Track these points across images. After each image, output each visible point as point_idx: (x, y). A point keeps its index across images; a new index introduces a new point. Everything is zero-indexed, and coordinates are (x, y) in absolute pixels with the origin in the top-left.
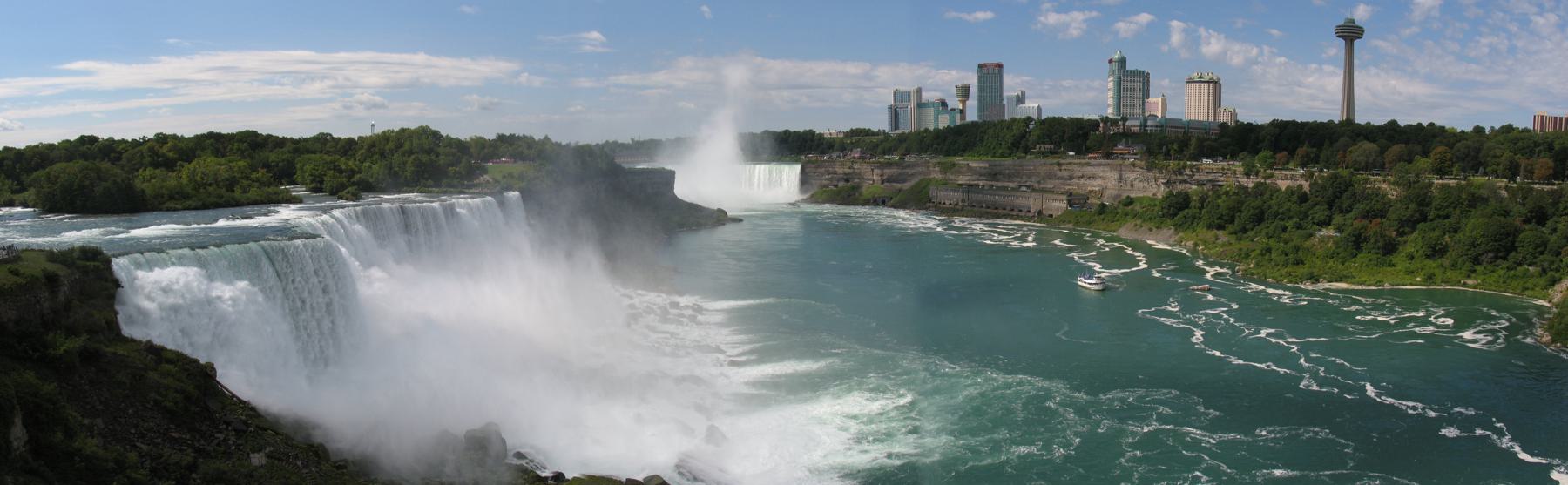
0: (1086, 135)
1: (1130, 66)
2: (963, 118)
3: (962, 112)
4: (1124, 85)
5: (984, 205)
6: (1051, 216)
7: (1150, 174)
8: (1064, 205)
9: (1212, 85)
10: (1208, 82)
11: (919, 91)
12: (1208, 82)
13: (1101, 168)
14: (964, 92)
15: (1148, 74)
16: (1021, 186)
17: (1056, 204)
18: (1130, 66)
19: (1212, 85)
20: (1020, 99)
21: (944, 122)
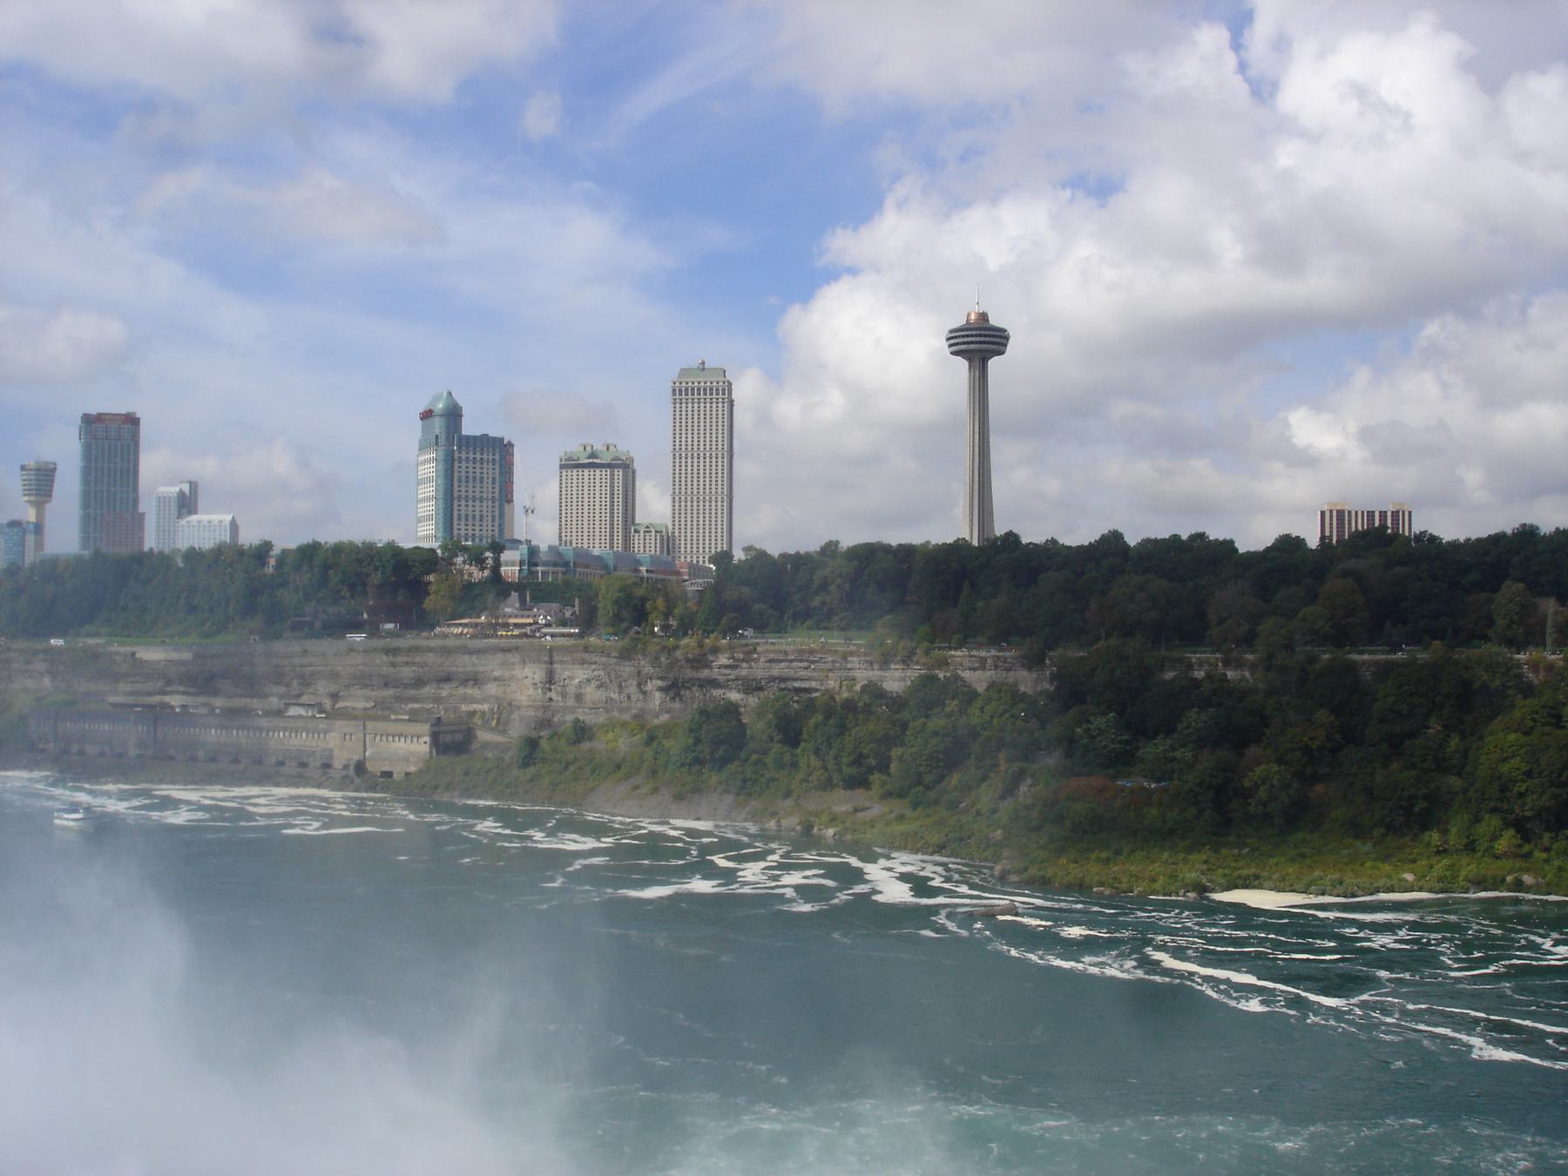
0: (418, 589)
1: (469, 428)
2: (39, 545)
3: (38, 528)
4: (461, 469)
5: (201, 754)
6: (389, 774)
7: (627, 669)
8: (422, 746)
9: (619, 473)
10: (609, 466)
12: (609, 466)
13: (500, 657)
14: (42, 481)
15: (510, 445)
16: (287, 705)
17: (401, 746)
18: (469, 428)
19: (619, 473)
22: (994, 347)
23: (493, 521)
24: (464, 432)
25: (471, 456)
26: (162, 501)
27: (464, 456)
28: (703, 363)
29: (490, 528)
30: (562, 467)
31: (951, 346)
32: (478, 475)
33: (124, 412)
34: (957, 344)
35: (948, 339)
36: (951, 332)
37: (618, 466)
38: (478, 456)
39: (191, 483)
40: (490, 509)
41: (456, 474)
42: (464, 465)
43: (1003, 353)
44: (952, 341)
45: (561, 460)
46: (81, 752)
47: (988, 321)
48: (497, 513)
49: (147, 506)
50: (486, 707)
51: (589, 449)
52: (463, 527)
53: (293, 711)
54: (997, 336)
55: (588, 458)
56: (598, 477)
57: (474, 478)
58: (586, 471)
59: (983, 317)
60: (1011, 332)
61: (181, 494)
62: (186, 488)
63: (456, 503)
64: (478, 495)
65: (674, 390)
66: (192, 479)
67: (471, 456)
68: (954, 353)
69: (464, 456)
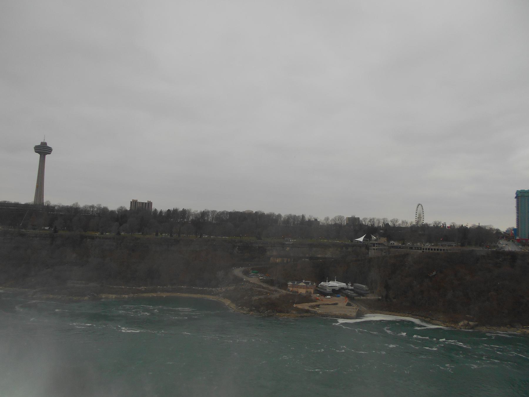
22: (48, 152)
31: (35, 150)
34: (36, 150)
35: (35, 148)
36: (36, 146)
43: (50, 154)
44: (36, 149)
47: (46, 145)
54: (49, 149)
59: (46, 144)
60: (53, 148)
68: (35, 152)
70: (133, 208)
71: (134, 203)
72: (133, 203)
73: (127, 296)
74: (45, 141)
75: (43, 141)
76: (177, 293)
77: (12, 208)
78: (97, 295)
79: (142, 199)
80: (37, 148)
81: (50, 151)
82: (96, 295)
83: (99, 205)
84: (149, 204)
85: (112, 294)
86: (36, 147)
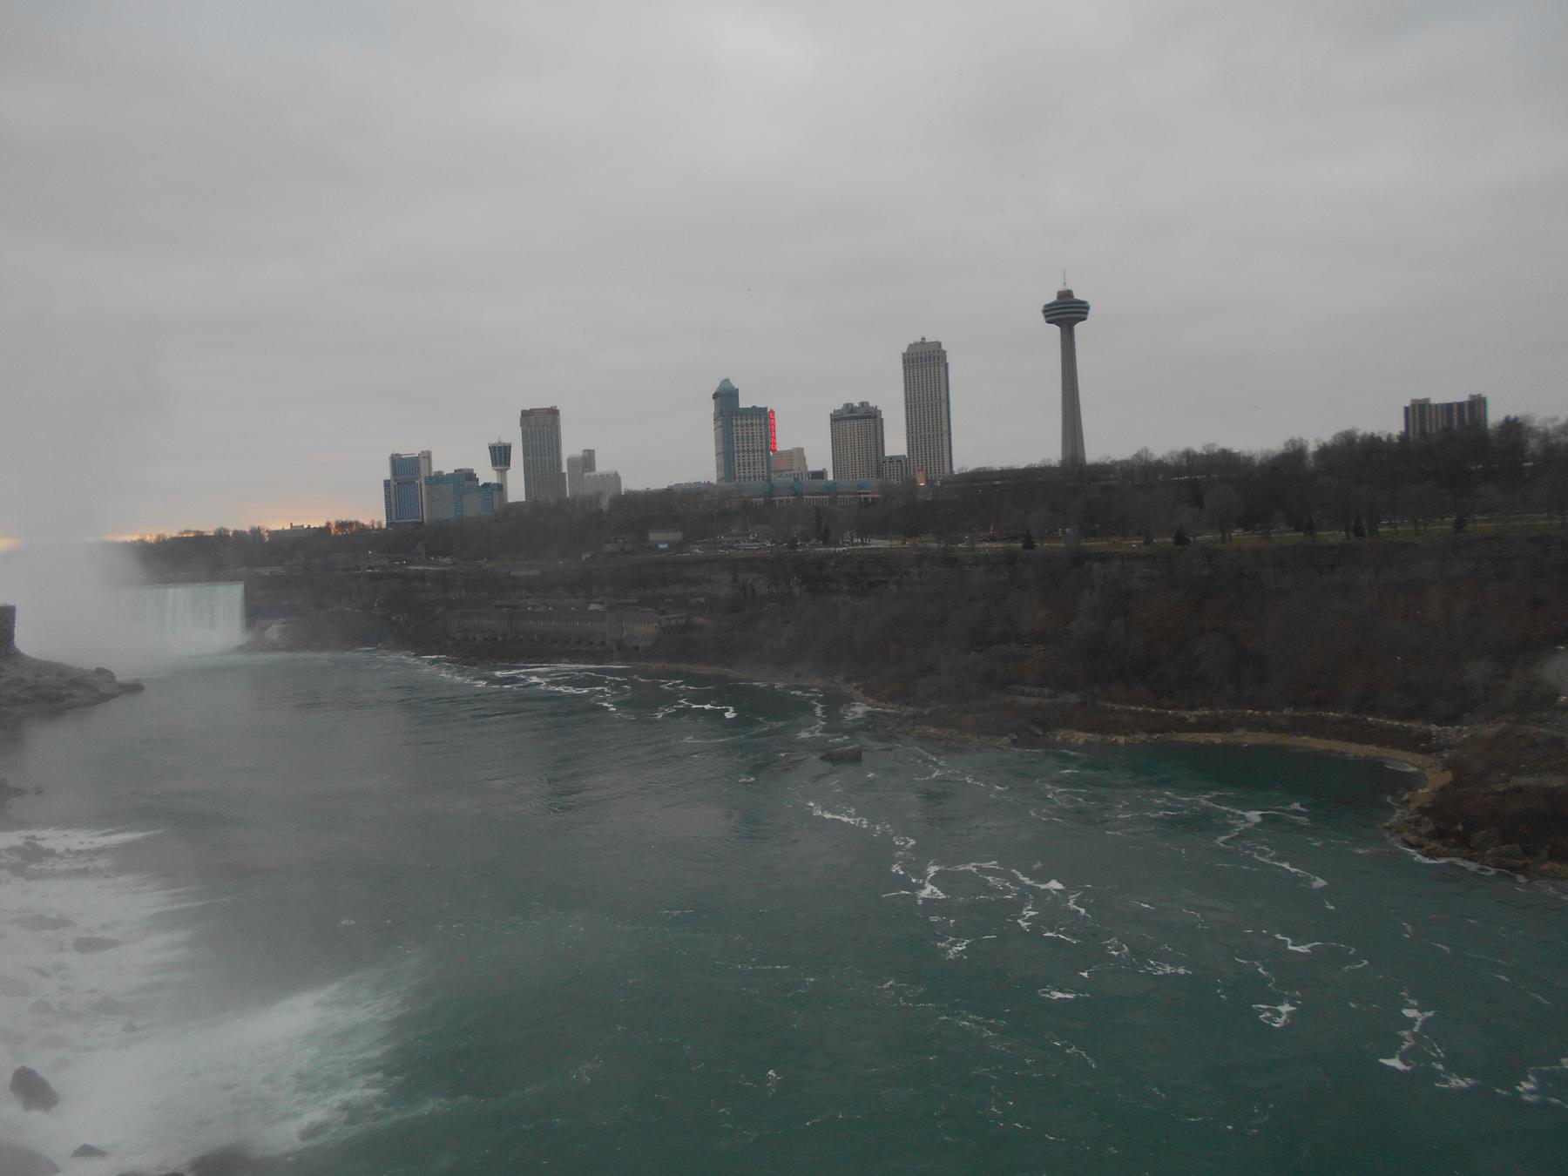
1: (744, 403)
3: (500, 488)
5: (536, 638)
6: (637, 648)
11: (427, 456)
14: (501, 455)
15: (772, 412)
16: (588, 603)
18: (744, 403)
20: (588, 460)
21: (473, 507)
23: (763, 465)
24: (740, 407)
25: (744, 422)
26: (571, 462)
27: (739, 422)
28: (924, 339)
29: (760, 470)
30: (832, 421)
31: (1046, 317)
32: (750, 435)
33: (549, 407)
35: (1044, 312)
36: (1046, 306)
37: (869, 417)
38: (749, 421)
39: (590, 450)
40: (760, 457)
41: (735, 435)
42: (739, 428)
43: (1085, 319)
44: (1047, 314)
45: (831, 415)
46: (474, 639)
48: (765, 460)
49: (565, 469)
50: (702, 600)
51: (850, 407)
52: (742, 471)
53: (593, 607)
54: (1079, 307)
55: (849, 413)
56: (856, 426)
57: (748, 437)
58: (848, 423)
60: (1091, 303)
61: (584, 458)
62: (587, 454)
63: (736, 455)
64: (751, 448)
65: (904, 363)
66: (588, 448)
67: (744, 422)
68: (1048, 322)
69: (739, 422)
70: (1431, 427)
71: (1418, 412)
72: (1414, 410)
73: (1121, 740)
74: (1069, 287)
75: (1061, 288)
76: (1303, 735)
77: (997, 483)
78: (1044, 731)
79: (1447, 391)
80: (1050, 310)
81: (1083, 310)
82: (1040, 733)
83: (1208, 445)
84: (1477, 405)
85: (1079, 730)
86: (1048, 308)
